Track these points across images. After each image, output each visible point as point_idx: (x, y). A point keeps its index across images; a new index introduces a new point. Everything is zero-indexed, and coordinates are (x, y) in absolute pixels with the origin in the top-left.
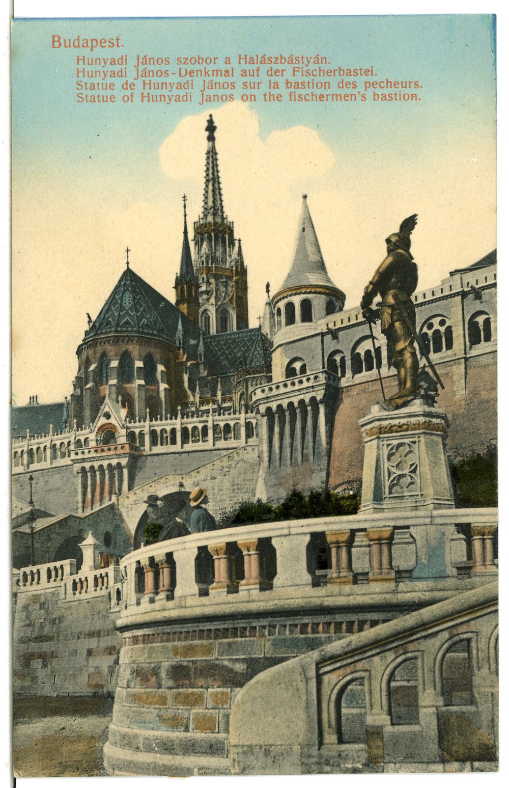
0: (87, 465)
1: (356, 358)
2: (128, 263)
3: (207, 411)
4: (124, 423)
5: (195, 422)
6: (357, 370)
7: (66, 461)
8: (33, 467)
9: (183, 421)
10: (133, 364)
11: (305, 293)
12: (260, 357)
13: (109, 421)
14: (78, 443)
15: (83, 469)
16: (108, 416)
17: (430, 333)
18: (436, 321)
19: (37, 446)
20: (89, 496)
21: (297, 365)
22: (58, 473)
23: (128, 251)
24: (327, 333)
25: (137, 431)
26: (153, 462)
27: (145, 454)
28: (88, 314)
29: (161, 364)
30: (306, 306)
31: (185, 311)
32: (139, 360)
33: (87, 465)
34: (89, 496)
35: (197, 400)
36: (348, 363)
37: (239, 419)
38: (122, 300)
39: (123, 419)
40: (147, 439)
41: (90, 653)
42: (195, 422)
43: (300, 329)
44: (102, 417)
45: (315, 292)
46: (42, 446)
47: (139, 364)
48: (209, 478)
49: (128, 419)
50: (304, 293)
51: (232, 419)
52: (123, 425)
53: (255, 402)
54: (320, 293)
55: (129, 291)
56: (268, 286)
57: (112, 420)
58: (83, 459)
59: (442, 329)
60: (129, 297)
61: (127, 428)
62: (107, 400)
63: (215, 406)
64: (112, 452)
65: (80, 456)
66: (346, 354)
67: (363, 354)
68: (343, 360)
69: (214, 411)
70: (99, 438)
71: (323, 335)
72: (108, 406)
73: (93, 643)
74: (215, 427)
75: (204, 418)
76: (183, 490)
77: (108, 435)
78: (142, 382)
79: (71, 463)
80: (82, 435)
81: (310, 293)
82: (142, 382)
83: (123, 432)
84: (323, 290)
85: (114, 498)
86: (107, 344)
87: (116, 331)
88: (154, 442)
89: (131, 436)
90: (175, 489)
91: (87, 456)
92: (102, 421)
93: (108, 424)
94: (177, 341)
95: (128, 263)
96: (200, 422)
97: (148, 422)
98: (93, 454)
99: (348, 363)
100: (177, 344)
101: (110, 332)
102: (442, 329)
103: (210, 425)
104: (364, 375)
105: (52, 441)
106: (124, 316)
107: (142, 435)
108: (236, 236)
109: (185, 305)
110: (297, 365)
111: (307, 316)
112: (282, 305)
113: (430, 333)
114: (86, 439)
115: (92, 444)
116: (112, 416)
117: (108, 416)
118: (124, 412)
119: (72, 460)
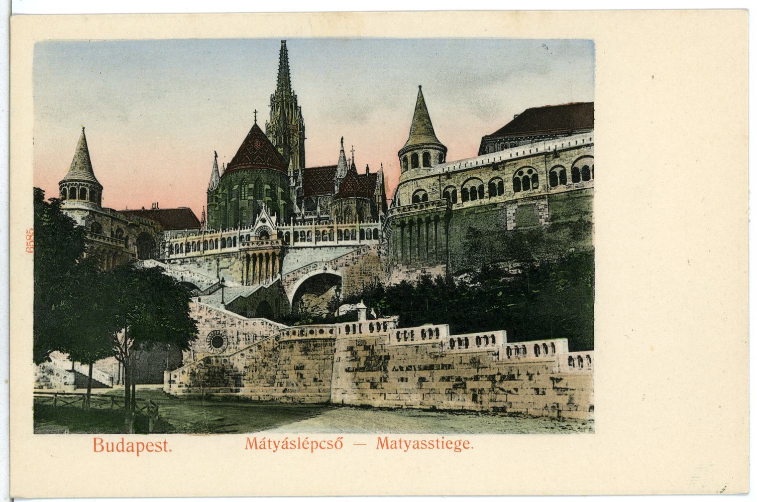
0: (251, 253)
1: (464, 191)
2: (256, 120)
3: (311, 220)
4: (275, 226)
5: (325, 227)
6: (465, 199)
7: (232, 249)
8: (208, 252)
9: (294, 227)
10: (261, 186)
11: (426, 148)
12: (350, 185)
13: (264, 224)
14: (241, 238)
15: (248, 256)
16: (264, 221)
17: (521, 178)
18: (525, 171)
19: (210, 238)
20: (251, 274)
21: (421, 195)
22: (227, 257)
23: (256, 112)
24: (444, 174)
25: (284, 232)
26: (296, 252)
27: (290, 246)
28: (215, 152)
29: (280, 187)
30: (427, 156)
31: (282, 153)
32: (268, 184)
33: (251, 253)
34: (251, 274)
35: (303, 212)
36: (459, 194)
37: (355, 226)
38: (254, 145)
39: (274, 223)
40: (292, 237)
41: (422, 380)
42: (325, 227)
43: (423, 171)
44: (260, 222)
45: (432, 148)
46: (214, 239)
47: (267, 187)
48: (344, 265)
49: (278, 224)
50: (425, 148)
51: (366, 226)
52: (275, 227)
53: (392, 217)
54: (436, 149)
55: (258, 138)
56: (342, 139)
57: (267, 224)
58: (248, 249)
59: (530, 176)
60: (259, 142)
61: (278, 229)
62: (263, 210)
63: (316, 217)
64: (269, 245)
65: (246, 246)
66: (457, 188)
67: (469, 189)
68: (455, 192)
69: (315, 219)
70: (257, 235)
71: (440, 175)
72: (264, 215)
73: (425, 374)
74: (339, 232)
75: (331, 225)
76: (327, 272)
77: (264, 234)
78: (270, 199)
79: (239, 250)
80: (245, 232)
81: (429, 148)
82: (270, 199)
83: (275, 232)
84: (437, 147)
85: (279, 276)
86: (246, 172)
87: (252, 164)
88: (295, 240)
89: (280, 235)
90: (321, 271)
91: (251, 246)
92: (260, 224)
93: (265, 226)
94: (289, 173)
95: (256, 120)
96: (328, 227)
97: (314, 225)
98: (255, 246)
99: (459, 194)
100: (289, 175)
101: (248, 165)
102: (530, 176)
103: (335, 229)
104: (469, 204)
105: (222, 236)
106: (256, 155)
107: (288, 233)
108: (299, 105)
109: (282, 149)
110: (421, 195)
111: (427, 163)
112: (409, 154)
113: (521, 178)
114: (248, 236)
115: (252, 239)
116: (267, 221)
117: (264, 221)
118: (274, 219)
119: (240, 249)
